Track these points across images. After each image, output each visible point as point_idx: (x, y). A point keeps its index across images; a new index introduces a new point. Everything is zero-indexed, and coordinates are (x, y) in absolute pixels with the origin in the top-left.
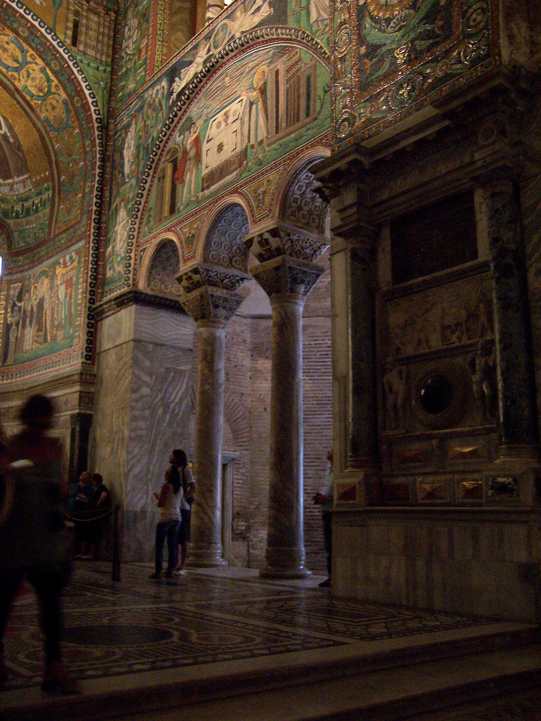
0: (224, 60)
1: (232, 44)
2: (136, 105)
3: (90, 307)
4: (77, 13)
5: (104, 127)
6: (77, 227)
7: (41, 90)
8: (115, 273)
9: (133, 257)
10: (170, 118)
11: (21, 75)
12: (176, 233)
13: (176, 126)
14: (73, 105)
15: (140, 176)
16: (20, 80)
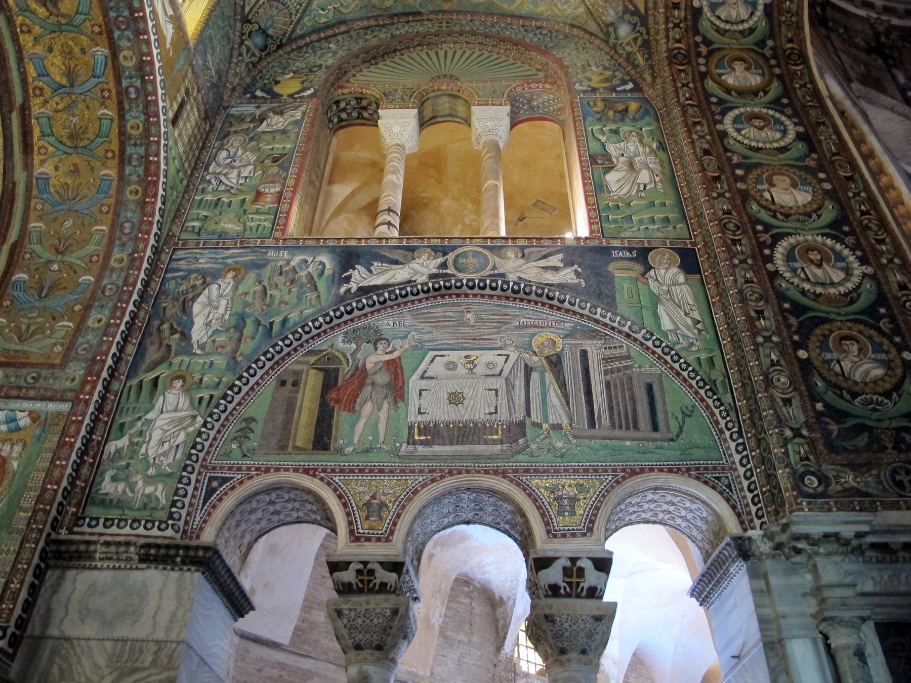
0: (469, 291)
1: (500, 282)
2: (240, 255)
3: (49, 535)
4: (187, 92)
5: (157, 251)
6: (44, 372)
7: (71, 137)
8: (133, 491)
9: (193, 482)
10: (338, 309)
11: (57, 99)
12: (329, 484)
13: (339, 325)
14: (120, 192)
15: (239, 359)
16: (46, 102)
